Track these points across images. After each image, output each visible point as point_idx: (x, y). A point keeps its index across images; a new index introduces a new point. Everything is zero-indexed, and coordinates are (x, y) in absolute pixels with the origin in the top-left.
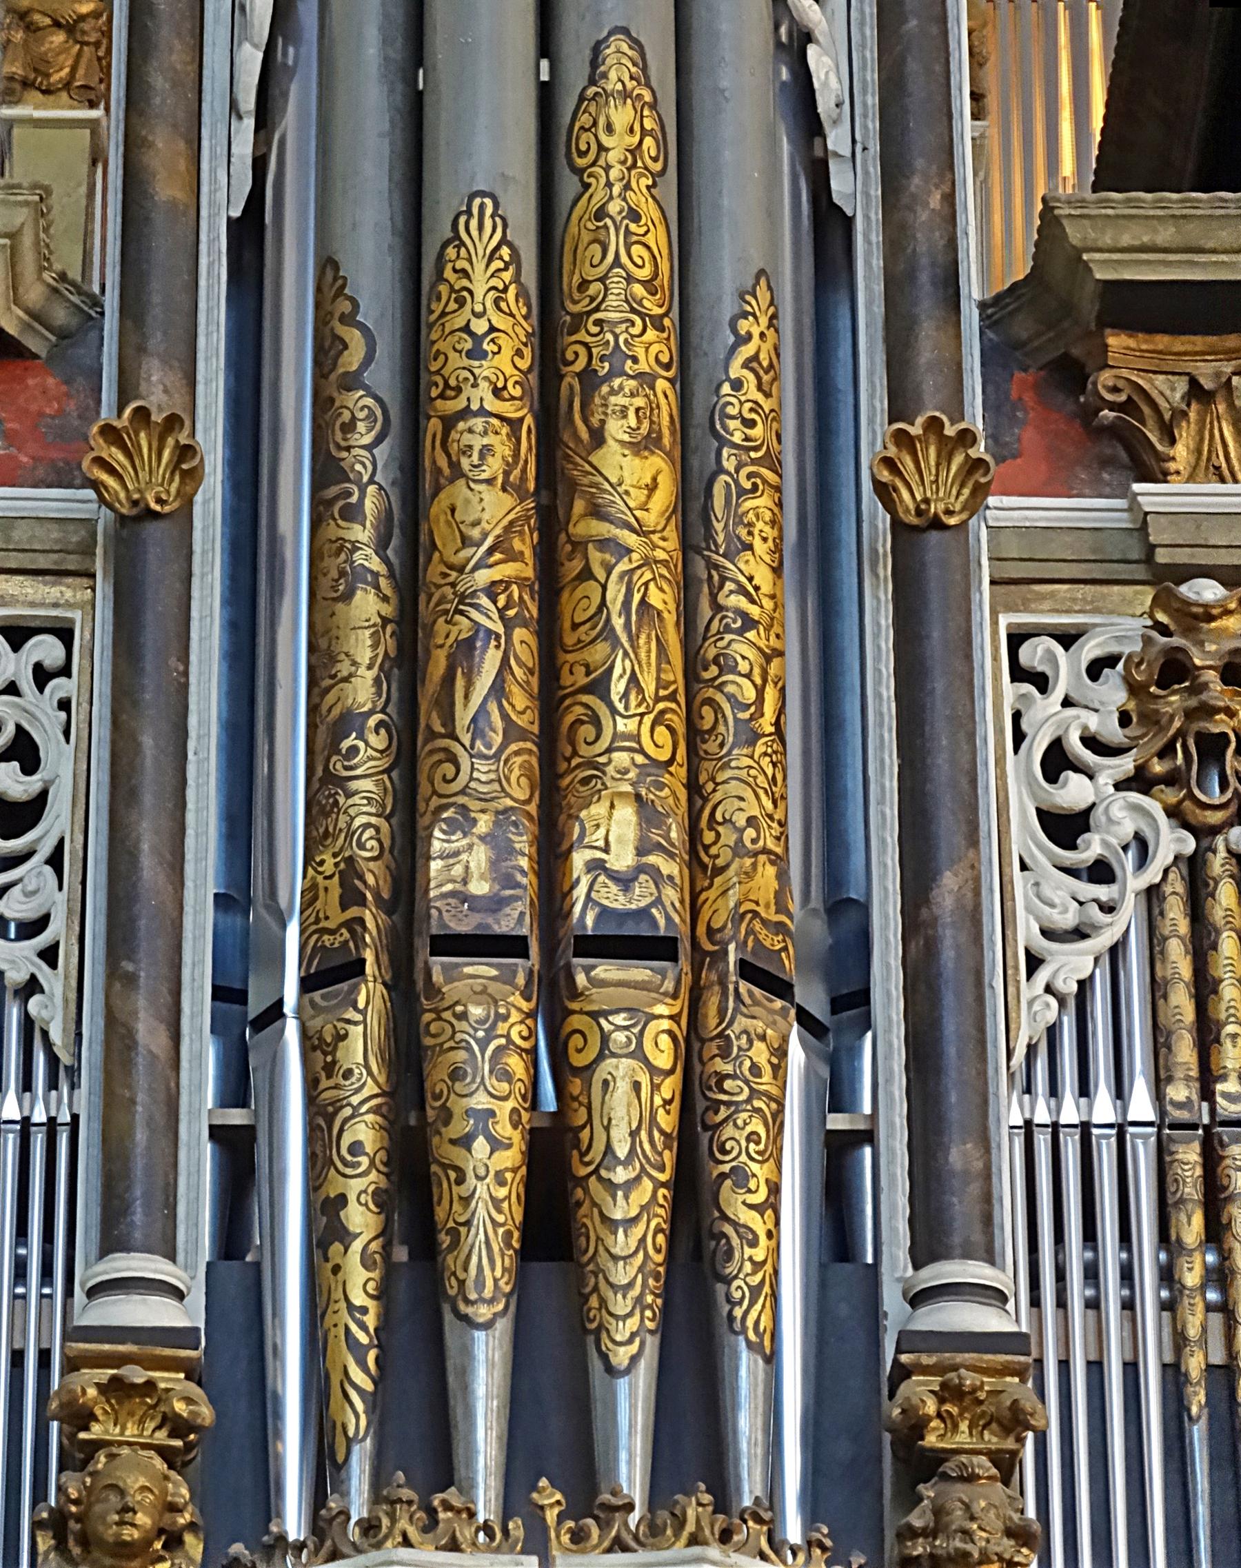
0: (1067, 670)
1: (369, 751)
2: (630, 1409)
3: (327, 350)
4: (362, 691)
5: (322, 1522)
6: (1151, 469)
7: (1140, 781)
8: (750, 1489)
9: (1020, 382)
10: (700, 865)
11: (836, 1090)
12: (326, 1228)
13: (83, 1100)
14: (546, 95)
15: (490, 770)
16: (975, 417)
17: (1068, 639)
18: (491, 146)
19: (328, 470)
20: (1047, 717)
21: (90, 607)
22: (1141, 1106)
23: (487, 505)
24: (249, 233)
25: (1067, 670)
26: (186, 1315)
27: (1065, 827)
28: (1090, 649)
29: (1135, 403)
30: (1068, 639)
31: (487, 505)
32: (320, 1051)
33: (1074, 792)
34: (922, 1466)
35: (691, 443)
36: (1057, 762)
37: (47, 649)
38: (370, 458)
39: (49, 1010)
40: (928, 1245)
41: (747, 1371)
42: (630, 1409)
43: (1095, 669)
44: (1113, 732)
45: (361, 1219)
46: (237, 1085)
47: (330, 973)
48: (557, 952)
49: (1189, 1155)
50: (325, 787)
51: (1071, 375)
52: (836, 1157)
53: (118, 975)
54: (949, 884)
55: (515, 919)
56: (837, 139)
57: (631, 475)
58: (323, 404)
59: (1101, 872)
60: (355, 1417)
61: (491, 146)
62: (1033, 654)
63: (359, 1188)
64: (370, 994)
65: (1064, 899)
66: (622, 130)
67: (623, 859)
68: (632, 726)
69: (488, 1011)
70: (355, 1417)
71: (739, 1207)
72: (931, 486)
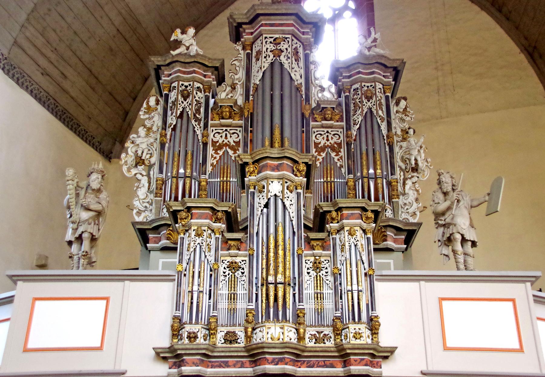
0: (309, 262)
1: (264, 271)
2: (280, 313)
3: (262, 243)
4: (264, 266)
5: (262, 321)
6: (314, 250)
8: (288, 319)
10: (285, 278)
11: (294, 290)
12: (262, 302)
13: (247, 292)
14: (276, 225)
15: (272, 272)
16: (303, 248)
18: (272, 230)
19: (262, 252)
20: (307, 266)
21: (247, 259)
22: (313, 292)
23: (272, 254)
24: (257, 233)
25: (309, 262)
26: (254, 307)
27: (308, 273)
29: (313, 245)
31: (272, 254)
32: (262, 290)
33: (309, 271)
34: (299, 316)
35: (284, 250)
36: (308, 269)
37: (244, 262)
38: (265, 251)
39: (245, 286)
40: (299, 302)
41: (288, 311)
42: (280, 313)
45: (264, 301)
46: (257, 291)
47: (262, 285)
48: (276, 284)
49: (316, 295)
50: (262, 273)
51: (309, 243)
52: (294, 295)
53: (249, 285)
54: (301, 278)
55: (273, 282)
56: (294, 227)
57: (281, 252)
58: (262, 247)
60: (264, 314)
61: (272, 230)
63: (264, 299)
64: (265, 287)
66: (280, 229)
67: (280, 278)
68: (281, 269)
69: (272, 287)
70: (264, 314)
71: (287, 300)
72: (300, 252)
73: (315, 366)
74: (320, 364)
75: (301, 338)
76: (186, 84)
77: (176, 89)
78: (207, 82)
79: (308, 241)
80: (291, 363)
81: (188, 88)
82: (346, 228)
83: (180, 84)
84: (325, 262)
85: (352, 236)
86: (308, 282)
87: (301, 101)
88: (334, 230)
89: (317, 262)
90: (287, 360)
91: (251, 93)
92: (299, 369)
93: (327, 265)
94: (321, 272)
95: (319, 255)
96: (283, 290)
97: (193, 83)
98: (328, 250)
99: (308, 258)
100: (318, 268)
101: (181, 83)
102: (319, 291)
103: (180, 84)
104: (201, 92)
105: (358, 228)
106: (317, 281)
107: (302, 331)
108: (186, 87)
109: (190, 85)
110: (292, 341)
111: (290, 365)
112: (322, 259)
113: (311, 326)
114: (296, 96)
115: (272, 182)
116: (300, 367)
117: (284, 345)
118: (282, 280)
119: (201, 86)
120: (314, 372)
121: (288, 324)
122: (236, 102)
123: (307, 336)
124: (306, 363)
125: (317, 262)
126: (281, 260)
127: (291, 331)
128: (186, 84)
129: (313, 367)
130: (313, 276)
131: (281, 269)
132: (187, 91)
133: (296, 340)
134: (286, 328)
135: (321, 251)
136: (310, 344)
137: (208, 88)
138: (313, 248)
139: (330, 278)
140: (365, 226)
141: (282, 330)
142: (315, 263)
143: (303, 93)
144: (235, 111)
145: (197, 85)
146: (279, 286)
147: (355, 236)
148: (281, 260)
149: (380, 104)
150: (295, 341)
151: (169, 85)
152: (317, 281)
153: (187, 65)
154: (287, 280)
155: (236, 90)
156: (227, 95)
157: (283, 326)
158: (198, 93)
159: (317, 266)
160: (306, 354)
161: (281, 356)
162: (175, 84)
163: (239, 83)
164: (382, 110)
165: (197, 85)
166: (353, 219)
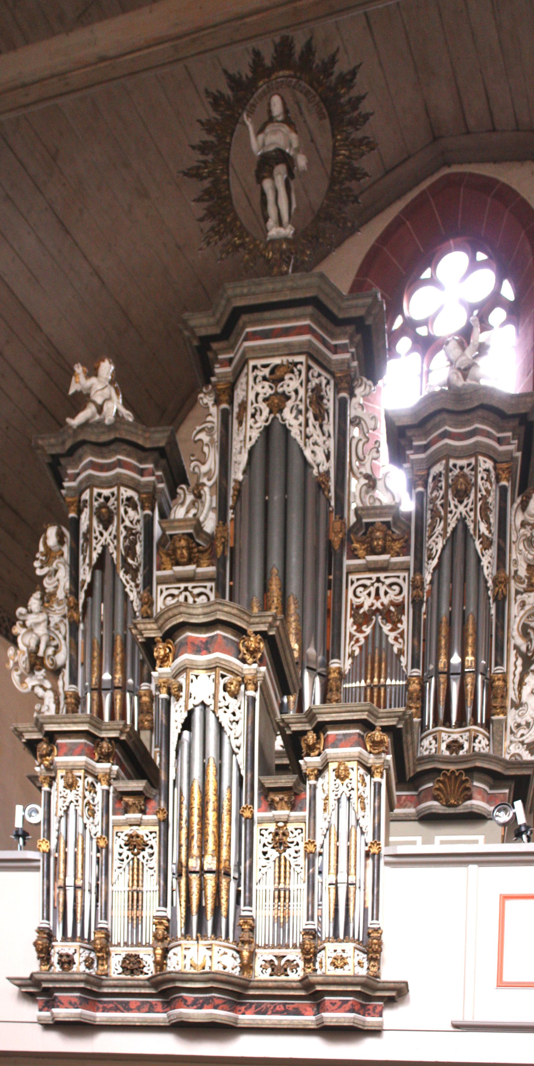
7: (273, 848)
9: (262, 797)
10: (219, 861)
17: (266, 830)
20: (264, 840)
27: (265, 853)
28: (268, 831)
29: (273, 801)
30: (266, 830)
33: (265, 849)
43: (270, 833)
44: (270, 842)
59: (268, 859)
62: (263, 832)
65: (265, 862)
68: (211, 846)
69: (195, 879)
73: (270, 1012)
75: (247, 966)
76: (106, 492)
77: (88, 505)
78: (147, 484)
79: (266, 791)
81: (110, 504)
82: (333, 766)
83: (95, 493)
84: (296, 833)
85: (342, 779)
86: (264, 870)
87: (328, 513)
88: (313, 771)
89: (281, 832)
90: (217, 1002)
91: (231, 503)
92: (241, 1017)
93: (297, 837)
94: (288, 850)
95: (285, 818)
96: (213, 884)
97: (119, 490)
98: (302, 809)
99: (265, 826)
100: (281, 844)
101: (96, 491)
102: (282, 886)
103: (95, 493)
104: (135, 508)
105: (354, 764)
106: (280, 867)
107: (246, 954)
108: (107, 499)
109: (113, 494)
110: (228, 970)
112: (290, 827)
113: (266, 947)
114: (317, 502)
116: (244, 1014)
117: (213, 977)
118: (214, 867)
119: (136, 497)
121: (217, 942)
122: (198, 526)
123: (258, 962)
124: (254, 1006)
125: (281, 832)
126: (211, 829)
127: (225, 953)
128: (106, 492)
129: (265, 1013)
130: (272, 859)
131: (211, 846)
132: (108, 508)
133: (238, 969)
134: (215, 949)
135: (287, 812)
136: (261, 974)
137: (149, 498)
138: (272, 806)
139: (302, 860)
140: (371, 760)
141: (209, 953)
142: (276, 834)
143: (332, 494)
145: (126, 493)
146: (208, 876)
147: (347, 781)
148: (211, 829)
149: (485, 509)
150: (237, 972)
151: (77, 499)
152: (280, 867)
154: (222, 865)
155: (203, 498)
156: (187, 512)
157: (211, 945)
158: (130, 510)
159: (280, 841)
160: (251, 992)
161: (208, 995)
162: (86, 496)
163: (209, 483)
164: (488, 522)
165: (126, 493)
166: (346, 746)
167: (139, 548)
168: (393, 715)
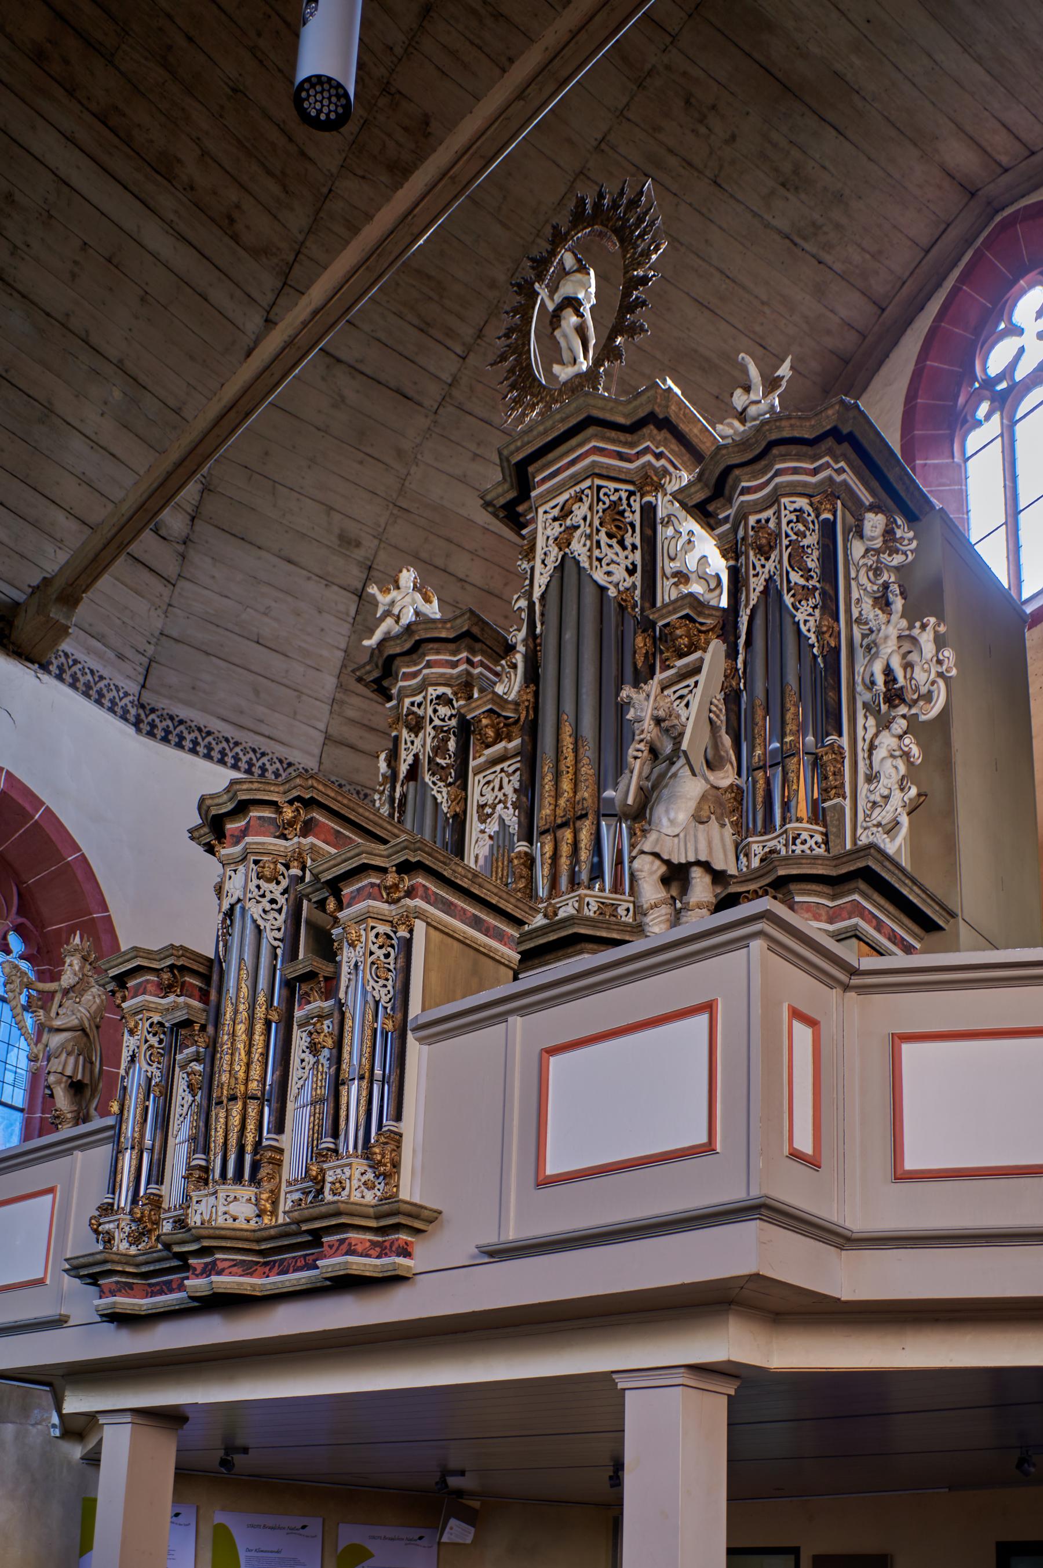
73: (291, 1269)
74: (299, 1264)
80: (234, 1269)
111: (230, 1274)
115: (235, 871)
120: (287, 1284)
129: (286, 1272)
144: (507, 718)
153: (414, 656)
167: (452, 745)
168: (398, 848)
